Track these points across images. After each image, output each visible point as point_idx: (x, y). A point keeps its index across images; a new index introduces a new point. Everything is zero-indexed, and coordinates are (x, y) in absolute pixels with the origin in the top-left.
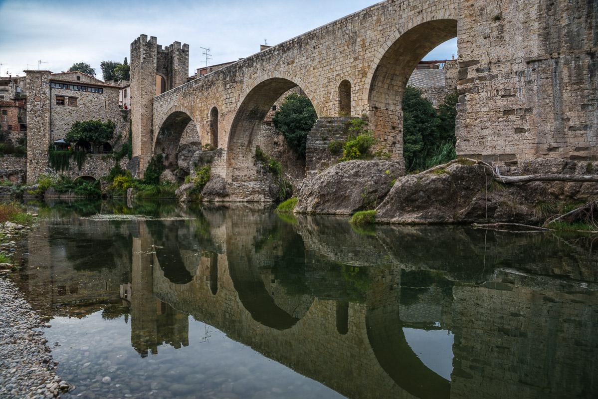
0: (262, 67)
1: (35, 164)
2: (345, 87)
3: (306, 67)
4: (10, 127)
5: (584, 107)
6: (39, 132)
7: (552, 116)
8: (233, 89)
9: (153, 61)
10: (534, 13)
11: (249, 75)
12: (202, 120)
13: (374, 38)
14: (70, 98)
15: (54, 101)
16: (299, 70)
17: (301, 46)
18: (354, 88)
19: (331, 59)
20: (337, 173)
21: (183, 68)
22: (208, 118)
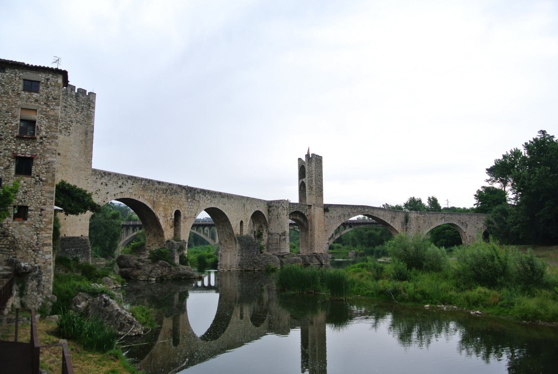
2: (242, 223)
3: (230, 209)
8: (193, 204)
17: (228, 199)
18: (244, 224)
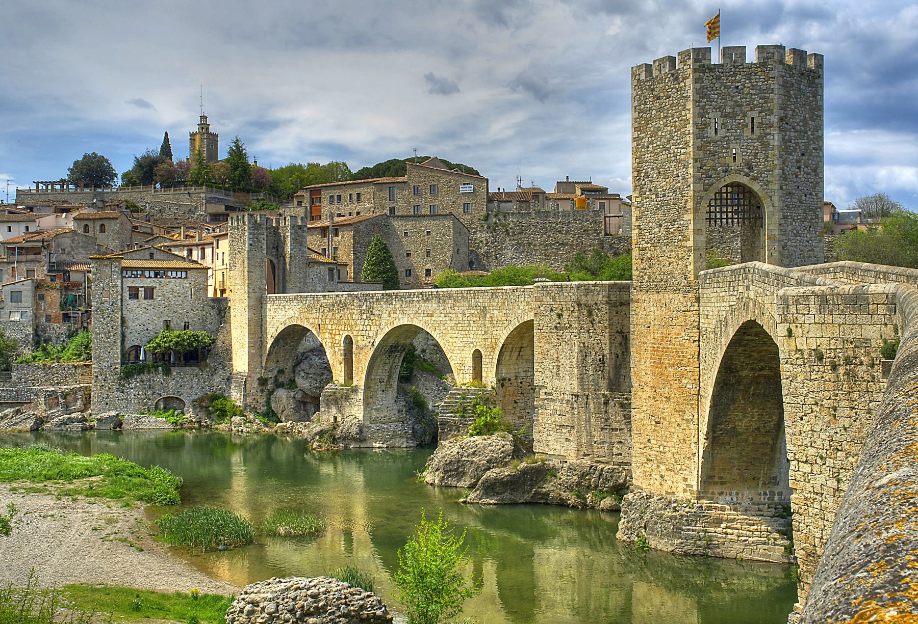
0: (402, 309)
1: (103, 381)
4: (49, 318)
5: (602, 429)
6: (108, 338)
7: (584, 434)
8: (370, 321)
9: (261, 247)
10: (575, 364)
11: (388, 312)
12: (332, 347)
13: (500, 319)
14: (146, 289)
15: (126, 295)
16: (437, 325)
17: (439, 302)
19: (466, 325)
20: (458, 453)
21: (300, 250)
22: (340, 346)
